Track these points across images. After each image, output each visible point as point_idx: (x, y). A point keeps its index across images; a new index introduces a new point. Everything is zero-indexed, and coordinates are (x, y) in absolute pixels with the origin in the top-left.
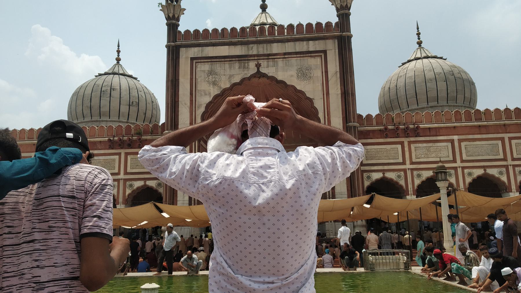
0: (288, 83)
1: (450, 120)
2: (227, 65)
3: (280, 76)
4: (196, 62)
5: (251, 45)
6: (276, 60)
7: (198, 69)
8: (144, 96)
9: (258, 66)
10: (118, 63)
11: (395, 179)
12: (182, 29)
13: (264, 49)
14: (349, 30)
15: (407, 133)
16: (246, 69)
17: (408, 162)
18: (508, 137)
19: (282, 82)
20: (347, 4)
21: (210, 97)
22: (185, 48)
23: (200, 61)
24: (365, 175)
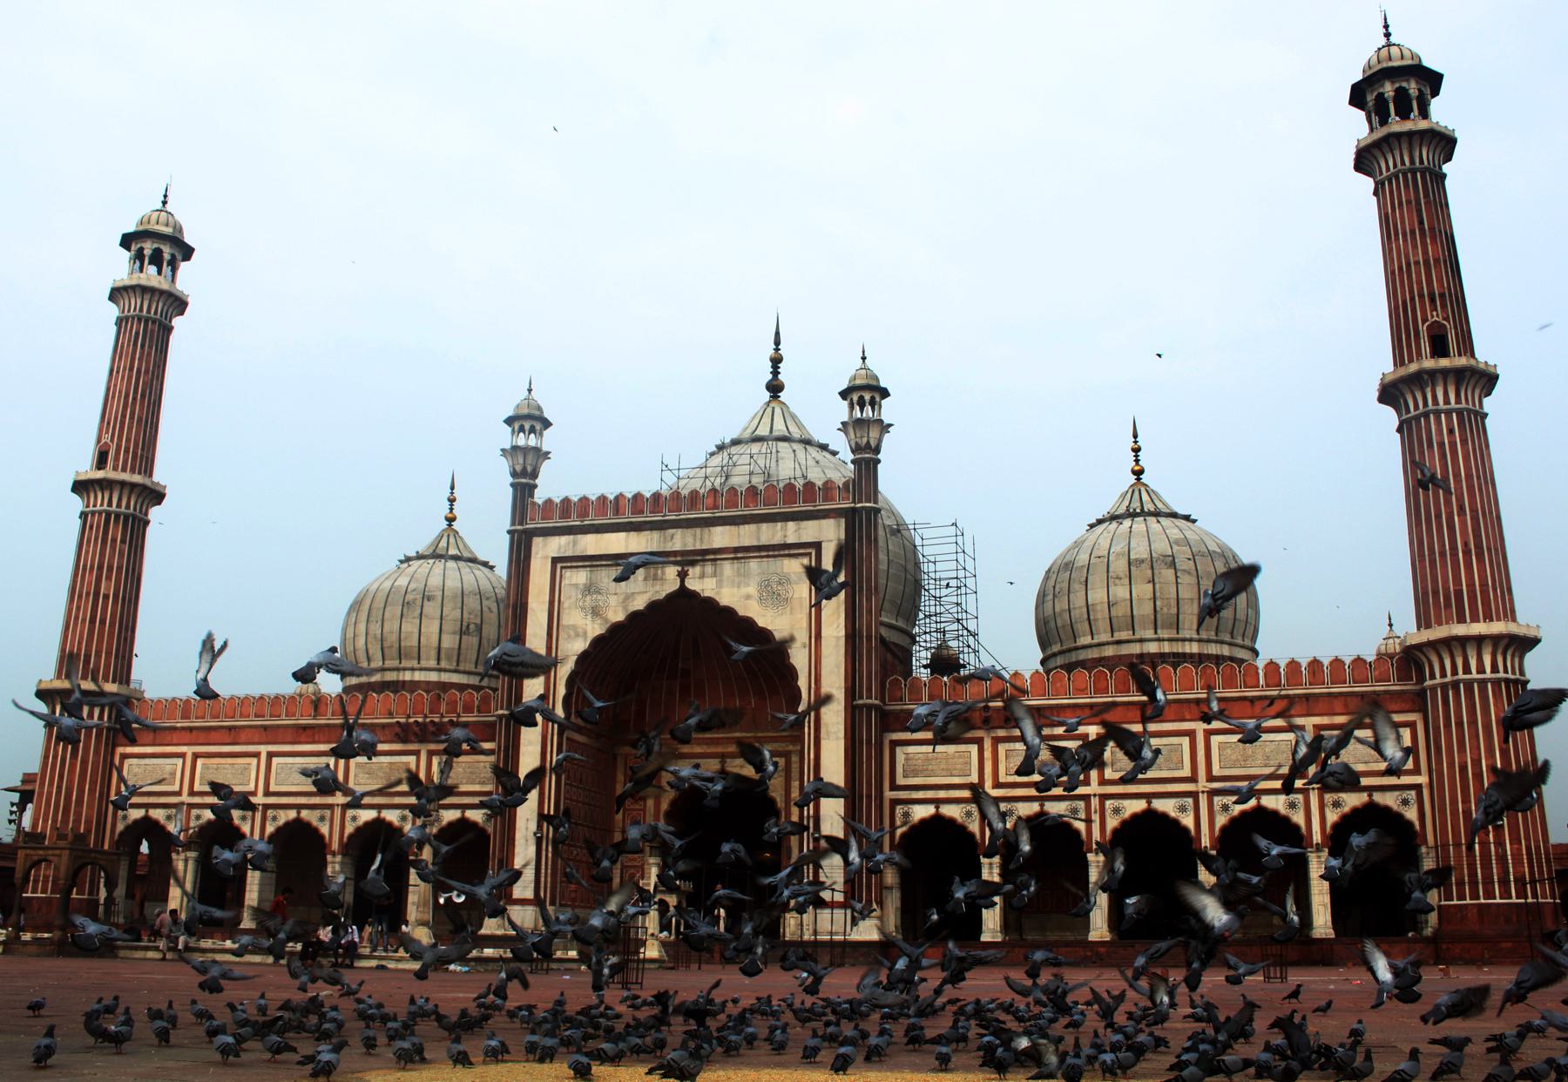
0: (741, 612)
1: (1083, 690)
4: (562, 568)
5: (671, 531)
6: (719, 562)
7: (566, 582)
8: (495, 610)
9: (683, 575)
10: (450, 525)
11: (960, 820)
12: (540, 496)
13: (695, 539)
16: (659, 582)
19: (729, 612)
20: (868, 442)
22: (541, 538)
23: (569, 564)
24: (899, 810)
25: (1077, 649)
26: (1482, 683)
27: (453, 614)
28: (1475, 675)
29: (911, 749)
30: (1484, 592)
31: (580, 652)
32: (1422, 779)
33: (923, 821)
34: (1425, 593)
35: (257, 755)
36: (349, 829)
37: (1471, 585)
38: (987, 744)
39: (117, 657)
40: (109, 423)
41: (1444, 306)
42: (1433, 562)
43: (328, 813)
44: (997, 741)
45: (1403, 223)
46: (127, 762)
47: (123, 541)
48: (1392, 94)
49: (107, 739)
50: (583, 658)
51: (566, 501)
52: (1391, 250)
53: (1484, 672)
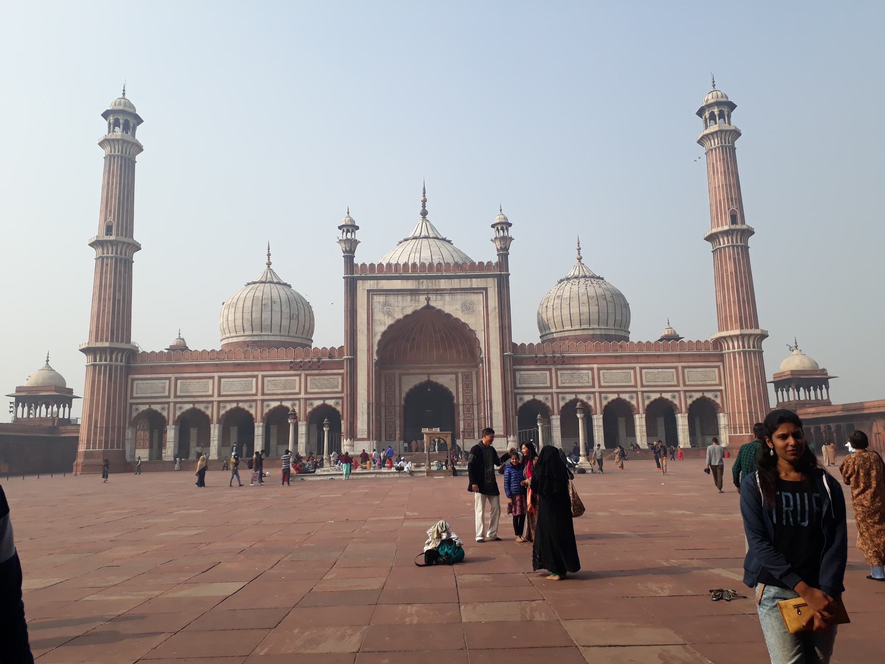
2: (400, 298)
3: (447, 309)
5: (421, 280)
7: (375, 300)
8: (302, 307)
9: (428, 299)
10: (269, 267)
14: (507, 271)
15: (554, 361)
17: (554, 386)
18: (640, 367)
19: (449, 315)
20: (506, 246)
21: (385, 326)
23: (375, 293)
24: (518, 397)
25: (564, 331)
26: (750, 352)
27: (286, 310)
28: (747, 349)
29: (522, 372)
30: (750, 317)
31: (383, 331)
32: (722, 388)
33: (528, 402)
34: (726, 317)
35: (213, 378)
36: (266, 410)
37: (745, 314)
38: (553, 371)
39: (126, 331)
40: (110, 211)
41: (736, 204)
42: (730, 305)
43: (254, 404)
44: (557, 370)
45: (721, 168)
46: (135, 383)
47: (125, 272)
48: (718, 112)
49: (125, 370)
50: (384, 334)
51: (372, 265)
52: (714, 178)
53: (750, 348)
